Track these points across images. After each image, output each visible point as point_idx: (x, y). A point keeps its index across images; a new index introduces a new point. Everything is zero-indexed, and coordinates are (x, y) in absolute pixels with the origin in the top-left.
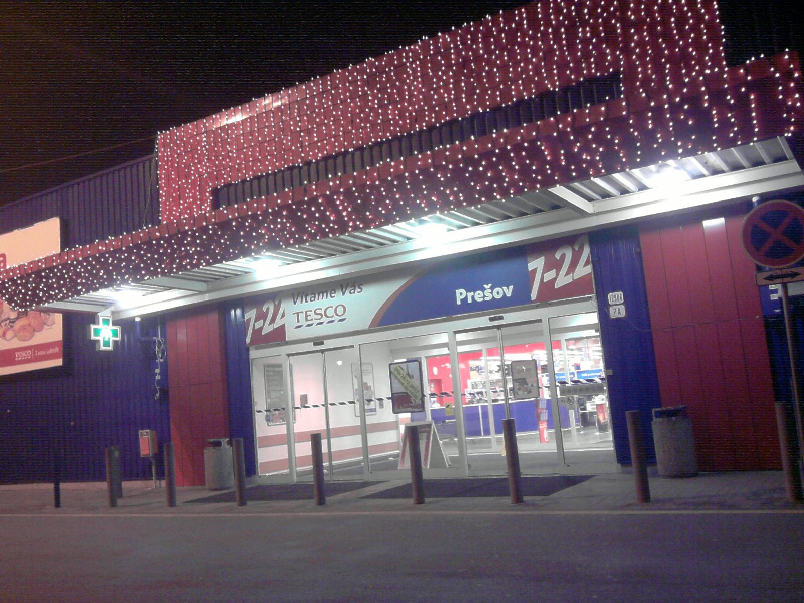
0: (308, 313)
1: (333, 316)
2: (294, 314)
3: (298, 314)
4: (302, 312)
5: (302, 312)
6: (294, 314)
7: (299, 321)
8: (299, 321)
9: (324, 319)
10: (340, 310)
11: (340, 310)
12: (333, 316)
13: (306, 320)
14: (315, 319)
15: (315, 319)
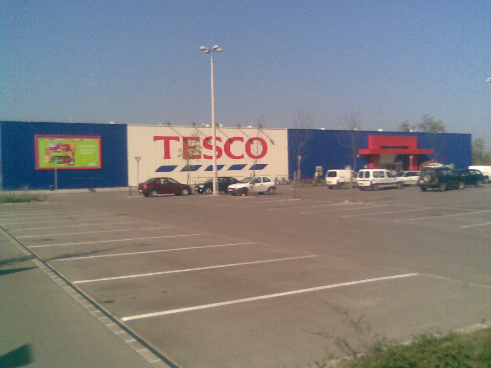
0: (191, 143)
1: (242, 157)
2: (156, 138)
3: (167, 140)
4: (177, 139)
5: (177, 139)
6: (156, 138)
7: (167, 155)
8: (167, 155)
9: (225, 160)
10: (256, 148)
11: (256, 148)
12: (242, 157)
13: (187, 156)
14: (206, 157)
15: (206, 157)
